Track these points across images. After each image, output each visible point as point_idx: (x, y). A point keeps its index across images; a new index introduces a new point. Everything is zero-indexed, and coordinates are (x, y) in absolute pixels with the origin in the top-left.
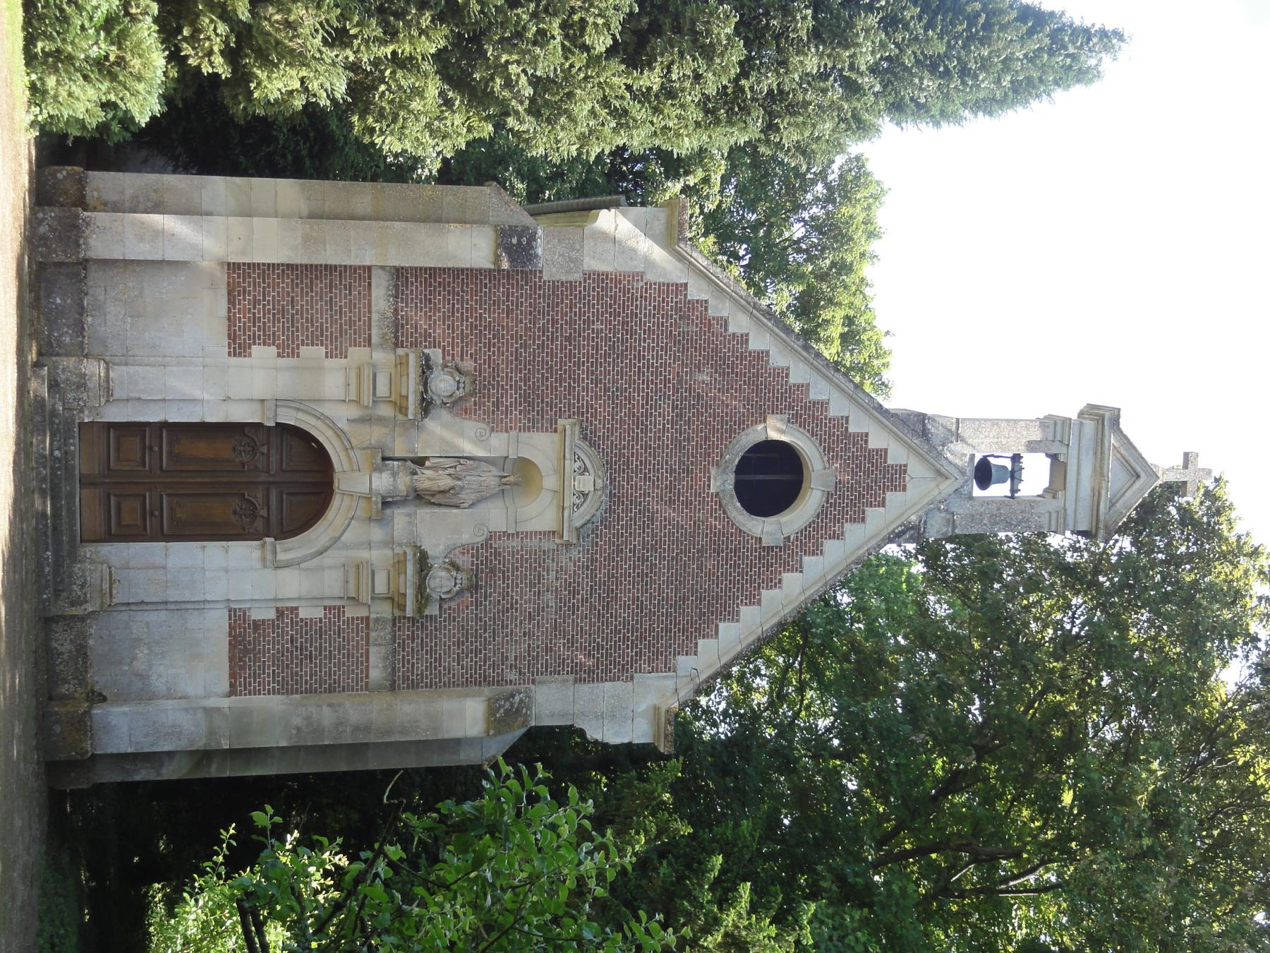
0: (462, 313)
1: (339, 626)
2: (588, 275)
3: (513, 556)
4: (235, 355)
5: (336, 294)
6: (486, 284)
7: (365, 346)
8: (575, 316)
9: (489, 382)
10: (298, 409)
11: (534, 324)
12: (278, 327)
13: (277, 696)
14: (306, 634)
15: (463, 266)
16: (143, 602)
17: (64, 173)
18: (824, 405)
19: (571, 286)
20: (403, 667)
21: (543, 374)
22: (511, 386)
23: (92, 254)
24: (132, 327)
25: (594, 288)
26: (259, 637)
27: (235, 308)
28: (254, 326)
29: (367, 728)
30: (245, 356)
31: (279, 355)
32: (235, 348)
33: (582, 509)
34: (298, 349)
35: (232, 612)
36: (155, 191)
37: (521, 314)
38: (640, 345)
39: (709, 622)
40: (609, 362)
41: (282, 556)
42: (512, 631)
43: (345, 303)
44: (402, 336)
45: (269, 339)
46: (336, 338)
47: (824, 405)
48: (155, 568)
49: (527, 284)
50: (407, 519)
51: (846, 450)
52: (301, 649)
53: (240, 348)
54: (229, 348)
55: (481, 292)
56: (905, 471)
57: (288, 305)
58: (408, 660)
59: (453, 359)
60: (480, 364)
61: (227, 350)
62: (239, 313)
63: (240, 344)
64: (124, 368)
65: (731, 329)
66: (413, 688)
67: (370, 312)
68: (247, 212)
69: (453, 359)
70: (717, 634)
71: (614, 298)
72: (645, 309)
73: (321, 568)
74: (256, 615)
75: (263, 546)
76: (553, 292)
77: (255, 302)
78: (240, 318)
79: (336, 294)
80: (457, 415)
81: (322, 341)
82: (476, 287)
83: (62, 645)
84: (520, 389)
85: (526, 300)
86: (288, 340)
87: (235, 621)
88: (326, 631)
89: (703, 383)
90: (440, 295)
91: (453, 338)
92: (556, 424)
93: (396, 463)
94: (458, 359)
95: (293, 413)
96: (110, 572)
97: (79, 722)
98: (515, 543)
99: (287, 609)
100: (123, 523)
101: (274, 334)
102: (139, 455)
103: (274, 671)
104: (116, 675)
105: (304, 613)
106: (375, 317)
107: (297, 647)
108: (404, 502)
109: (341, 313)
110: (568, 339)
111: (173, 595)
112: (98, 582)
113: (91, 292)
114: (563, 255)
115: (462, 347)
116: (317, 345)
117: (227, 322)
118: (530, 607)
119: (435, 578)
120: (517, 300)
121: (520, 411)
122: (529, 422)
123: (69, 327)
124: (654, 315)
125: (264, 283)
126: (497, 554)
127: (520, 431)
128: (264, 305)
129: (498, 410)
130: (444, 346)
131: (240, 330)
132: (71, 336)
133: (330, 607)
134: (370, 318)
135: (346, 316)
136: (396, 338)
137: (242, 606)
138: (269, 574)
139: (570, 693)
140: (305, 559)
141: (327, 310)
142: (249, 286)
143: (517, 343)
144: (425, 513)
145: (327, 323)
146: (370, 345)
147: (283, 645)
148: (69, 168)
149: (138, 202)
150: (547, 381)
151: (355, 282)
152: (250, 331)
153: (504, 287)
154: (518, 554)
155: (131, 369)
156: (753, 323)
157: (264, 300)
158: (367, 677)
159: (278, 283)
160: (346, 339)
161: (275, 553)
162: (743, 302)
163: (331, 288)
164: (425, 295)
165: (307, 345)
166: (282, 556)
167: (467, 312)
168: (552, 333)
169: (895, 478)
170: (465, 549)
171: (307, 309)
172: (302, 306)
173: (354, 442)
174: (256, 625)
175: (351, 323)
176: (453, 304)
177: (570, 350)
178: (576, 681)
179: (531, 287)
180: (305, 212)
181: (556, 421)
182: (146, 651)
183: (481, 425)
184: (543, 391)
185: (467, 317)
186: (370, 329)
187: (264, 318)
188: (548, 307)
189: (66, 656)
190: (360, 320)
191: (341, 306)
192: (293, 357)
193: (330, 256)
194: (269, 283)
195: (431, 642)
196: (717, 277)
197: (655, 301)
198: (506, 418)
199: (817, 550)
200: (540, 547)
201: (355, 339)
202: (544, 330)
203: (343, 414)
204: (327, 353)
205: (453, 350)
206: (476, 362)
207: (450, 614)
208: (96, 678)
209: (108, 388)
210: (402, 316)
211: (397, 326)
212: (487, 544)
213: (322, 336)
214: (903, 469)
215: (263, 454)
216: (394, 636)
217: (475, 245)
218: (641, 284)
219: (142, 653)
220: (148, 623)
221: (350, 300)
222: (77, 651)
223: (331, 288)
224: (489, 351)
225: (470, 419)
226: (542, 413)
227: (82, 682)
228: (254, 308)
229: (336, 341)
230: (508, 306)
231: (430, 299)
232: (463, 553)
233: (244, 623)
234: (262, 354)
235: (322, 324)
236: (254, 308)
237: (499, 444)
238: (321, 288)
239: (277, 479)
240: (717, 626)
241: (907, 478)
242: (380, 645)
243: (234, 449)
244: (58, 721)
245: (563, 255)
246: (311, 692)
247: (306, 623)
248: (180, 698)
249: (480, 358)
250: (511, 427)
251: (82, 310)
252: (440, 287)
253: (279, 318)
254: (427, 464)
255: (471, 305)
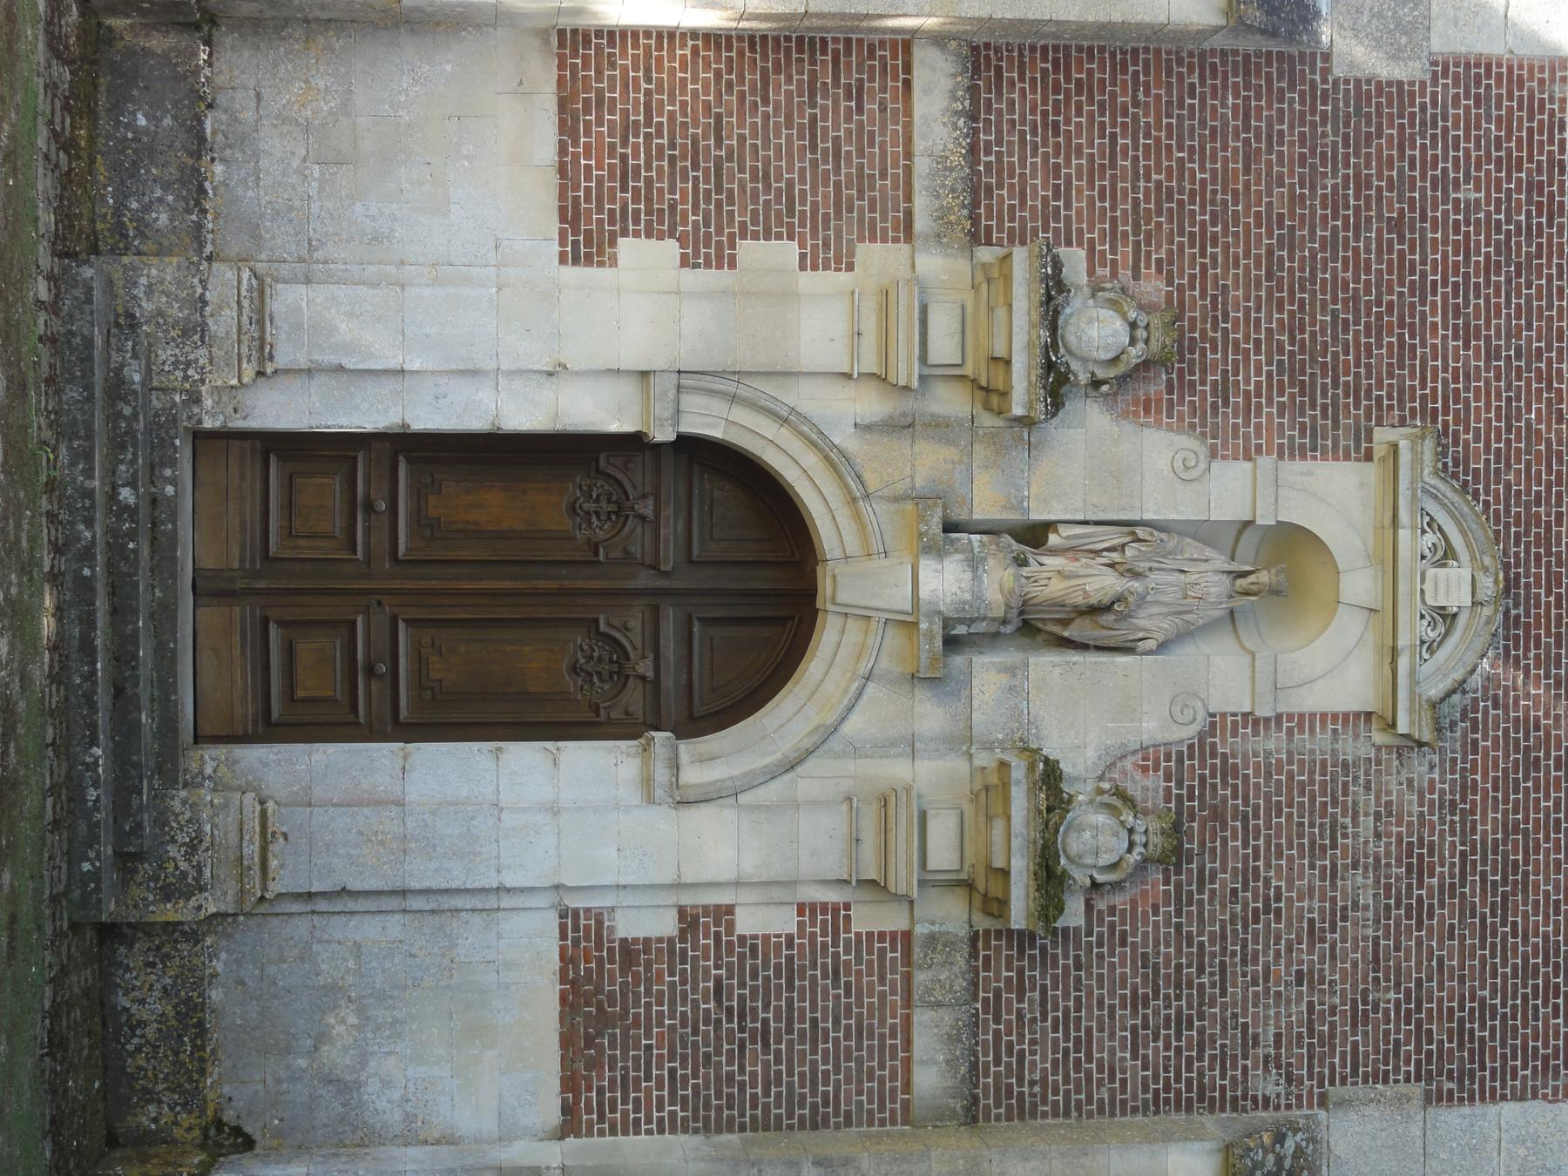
0: (1136, 158)
1: (836, 955)
2: (1441, 67)
3: (1269, 775)
4: (576, 261)
5: (824, 109)
7: (896, 240)
8: (1412, 167)
9: (1203, 332)
10: (733, 398)
11: (1313, 188)
12: (684, 192)
13: (682, 1138)
16: (344, 892)
19: (1400, 92)
20: (997, 1062)
21: (1335, 314)
22: (1257, 342)
24: (321, 189)
25: (1456, 97)
26: (637, 983)
27: (575, 144)
28: (624, 189)
30: (601, 264)
31: (684, 262)
32: (575, 244)
33: (1442, 654)
34: (733, 246)
35: (569, 920)
37: (1281, 163)
43: (849, 132)
44: (989, 217)
45: (661, 222)
46: (826, 217)
48: (379, 803)
49: (1292, 88)
50: (1004, 679)
52: (742, 1017)
53: (588, 243)
54: (563, 243)
55: (1181, 107)
57: (706, 137)
58: (1010, 1045)
59: (1114, 274)
60: (1181, 288)
62: (588, 156)
63: (588, 233)
66: (1021, 1117)
67: (909, 155)
69: (1114, 274)
71: (1506, 123)
76: (1358, 108)
78: (588, 168)
79: (824, 109)
80: (1125, 415)
81: (791, 226)
82: (1169, 93)
84: (1281, 351)
85: (1291, 127)
86: (707, 224)
87: (576, 942)
88: (802, 969)
90: (1079, 113)
91: (1114, 220)
92: (1369, 439)
94: (1125, 274)
95: (718, 407)
96: (264, 814)
98: (1274, 742)
99: (706, 910)
100: (300, 694)
101: (672, 207)
103: (672, 1071)
104: (278, 1081)
105: (747, 923)
106: (921, 165)
107: (730, 1010)
108: (993, 639)
109: (837, 156)
110: (1397, 225)
111: (422, 872)
112: (233, 838)
113: (222, 100)
115: (1137, 244)
116: (779, 237)
118: (1312, 908)
119: (1081, 829)
120: (1270, 126)
121: (1281, 406)
123: (166, 187)
126: (1228, 771)
127: (1281, 456)
128: (648, 136)
129: (1226, 404)
130: (1091, 242)
131: (588, 199)
132: (172, 209)
133: (813, 907)
134: (908, 170)
135: (849, 164)
136: (974, 219)
137: (595, 902)
138: (662, 822)
141: (802, 149)
143: (1270, 235)
145: (803, 181)
150: (1346, 330)
152: (612, 200)
153: (1236, 95)
157: (648, 123)
159: (683, 81)
160: (850, 221)
161: (675, 766)
163: (812, 95)
164: (1045, 114)
165: (755, 236)
166: (693, 777)
168: (1357, 209)
170: (1150, 757)
171: (754, 147)
172: (742, 138)
173: (873, 483)
174: (630, 952)
176: (1113, 136)
177: (1401, 253)
178: (1428, 1100)
179: (1302, 94)
181: (1369, 432)
182: (353, 1020)
184: (1335, 355)
186: (909, 198)
187: (649, 168)
188: (1346, 145)
189: (150, 1031)
190: (883, 176)
192: (720, 267)
195: (1066, 996)
198: (1247, 424)
201: (873, 222)
202: (1335, 203)
204: (803, 257)
205: (1114, 251)
206: (1170, 283)
207: (1112, 926)
208: (226, 1089)
209: (262, 339)
210: (988, 165)
211: (976, 192)
212: (1201, 746)
213: (791, 213)
215: (643, 518)
216: (974, 984)
219: (342, 1025)
221: (860, 125)
223: (812, 95)
224: (1203, 254)
225: (1159, 424)
226: (1333, 412)
227: (191, 1097)
228: (624, 144)
230: (1247, 142)
231: (1056, 124)
232: (1145, 769)
233: (599, 947)
235: (790, 184)
236: (624, 144)
238: (789, 94)
239: (678, 584)
242: (939, 1005)
243: (572, 509)
246: (766, 1128)
248: (438, 1142)
249: (1181, 270)
250: (1259, 449)
251: (199, 144)
252: (1079, 93)
253: (684, 170)
254: (1053, 539)
255: (1158, 140)
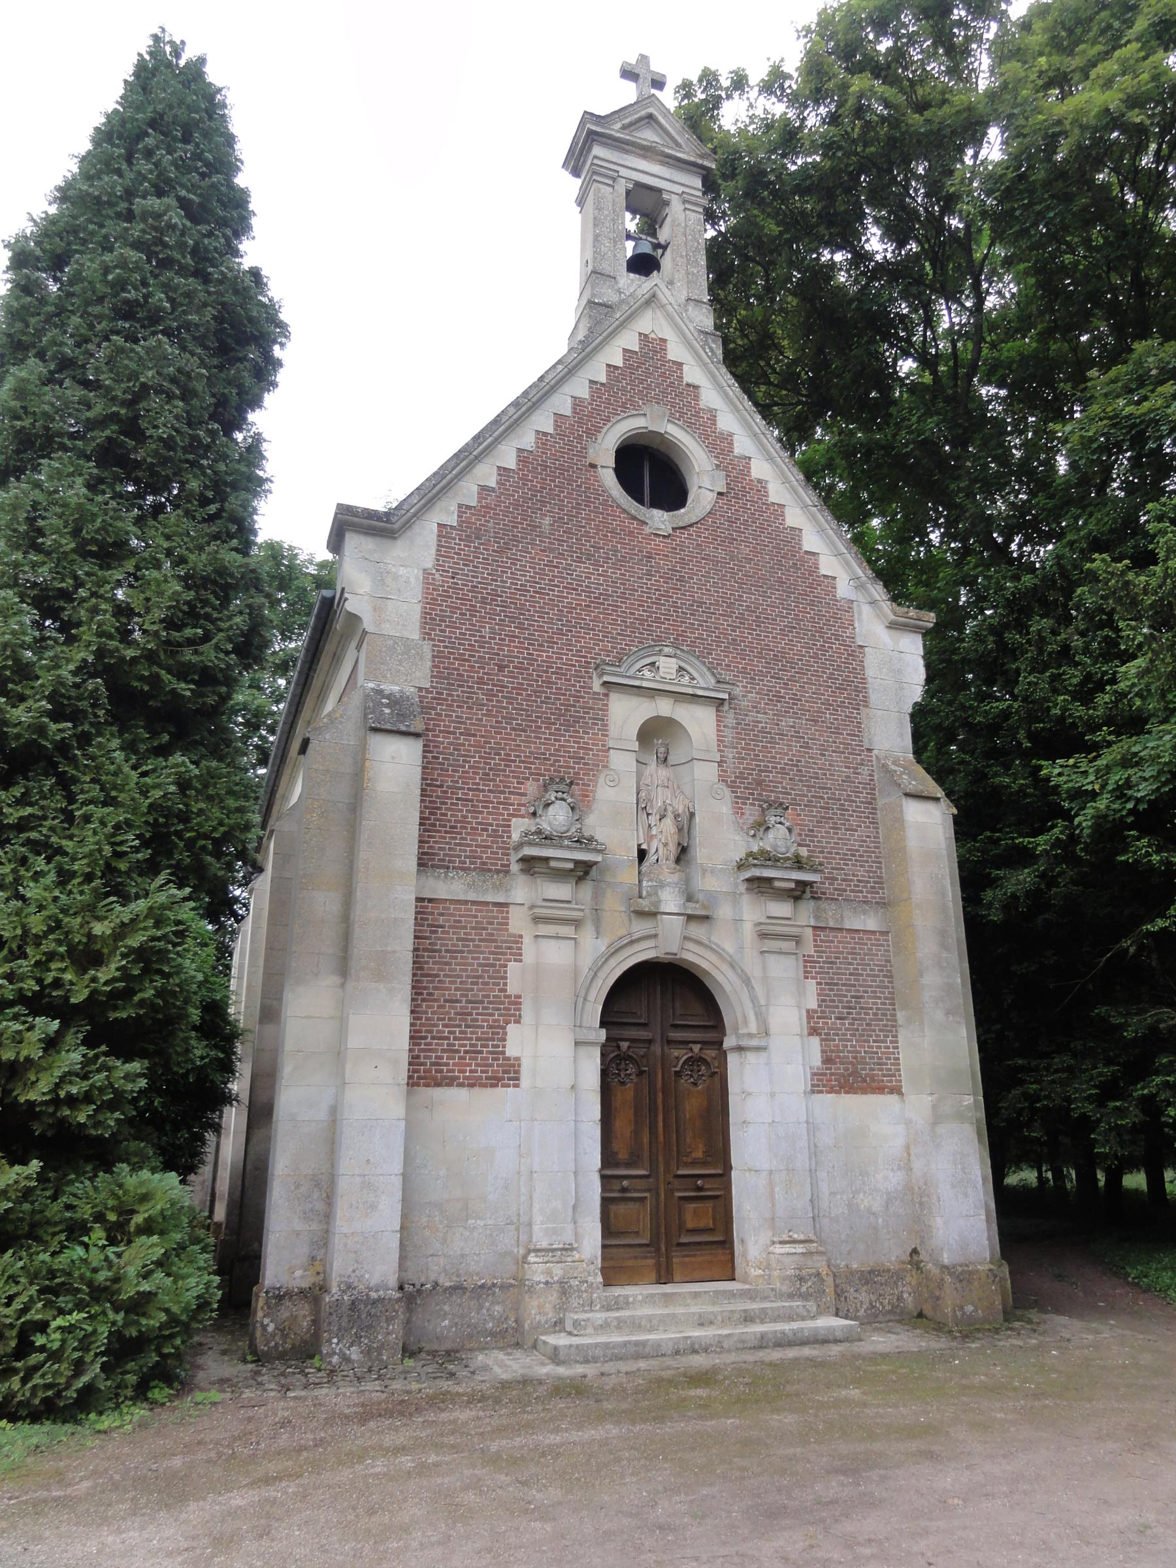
0: (469, 789)
1: (824, 962)
2: (426, 635)
3: (743, 758)
4: (517, 1079)
5: (442, 945)
6: (434, 757)
7: (508, 912)
8: (473, 656)
9: (551, 765)
10: (585, 999)
11: (483, 705)
12: (483, 1021)
13: (900, 1038)
14: (834, 1001)
15: (419, 777)
16: (811, 1201)
17: (266, 1321)
18: (577, 402)
19: (437, 656)
20: (861, 892)
21: (542, 702)
22: (556, 740)
23: (393, 1281)
24: (480, 1218)
25: (441, 631)
26: (839, 1057)
27: (458, 1078)
28: (481, 1052)
29: (943, 933)
30: (519, 1066)
31: (518, 1022)
32: (509, 1079)
33: (695, 674)
34: (509, 997)
35: (815, 1089)
36: (297, 1187)
37: (471, 719)
38: (509, 588)
39: (801, 559)
40: (529, 625)
41: (753, 1027)
42: (820, 769)
43: (454, 933)
44: (496, 864)
45: (498, 1033)
46: (496, 947)
47: (577, 402)
48: (771, 1185)
49: (434, 709)
50: (708, 875)
51: (624, 389)
52: (850, 1008)
53: (508, 1072)
54: (508, 1086)
55: (443, 764)
56: (646, 336)
57: (455, 1008)
58: (855, 886)
59: (523, 805)
60: (531, 774)
61: (511, 1089)
62: (464, 1071)
63: (504, 1072)
64: (536, 1228)
65: (492, 483)
66: (882, 883)
67: (466, 902)
68: (338, 1054)
69: (523, 805)
70: (813, 554)
71: (453, 609)
72: (467, 575)
73: (765, 979)
74: (817, 1060)
75: (740, 1049)
76: (445, 678)
77: (452, 1051)
78: (471, 1071)
79: (442, 945)
80: (589, 806)
81: (501, 966)
82: (437, 769)
83: (861, 1302)
84: (559, 730)
85: (454, 711)
86: (499, 1009)
87: (824, 1086)
88: (830, 978)
89: (552, 525)
90: (446, 815)
91: (498, 803)
92: (598, 694)
93: (645, 883)
94: (524, 800)
95: (589, 1006)
96: (781, 1243)
97: (961, 1281)
98: (730, 754)
99: (809, 1023)
100: (711, 1226)
101: (491, 1027)
102: (632, 1206)
103: (874, 1041)
104: (889, 1232)
105: (813, 1004)
106: (472, 896)
107: (848, 1013)
108: (687, 881)
109: (467, 940)
110: (501, 668)
111: (802, 1161)
112: (795, 1258)
113: (433, 1277)
114: (401, 662)
115: (510, 793)
116: (506, 972)
117: (477, 1089)
118: (796, 746)
119: (776, 846)
120: (453, 722)
121: (584, 732)
122: (597, 724)
123: (481, 1307)
124: (474, 566)
125: (425, 1038)
126: (741, 776)
127: (607, 736)
128: (455, 1039)
129: (583, 758)
130: (509, 815)
131: (487, 1072)
132: (492, 1303)
133: (805, 972)
134: (474, 903)
135: (469, 934)
136: (498, 872)
137: (809, 1076)
138: (775, 1043)
139: (879, 713)
140: (754, 1000)
141: (462, 958)
142: (430, 1057)
143: (506, 728)
144: (701, 854)
145: (478, 958)
146: (506, 905)
147: (846, 1029)
148: (260, 1314)
149: (312, 1210)
150: (550, 698)
151: (427, 919)
152: (487, 1059)
153: (438, 736)
154: (741, 753)
155: (538, 1219)
156: (485, 460)
157: (448, 1038)
158: (873, 932)
159: (427, 1019)
160: (498, 935)
161: (750, 1036)
162: (464, 463)
163: (435, 951)
164: (446, 832)
165: (505, 984)
166: (753, 1027)
167: (467, 784)
168: (493, 685)
169: (652, 347)
170: (738, 811)
171: (461, 983)
172: (457, 989)
173: (623, 932)
174: (827, 1060)
175: (478, 928)
176: (458, 799)
177: (514, 667)
178: (867, 706)
179: (438, 704)
180: (335, 979)
181: (595, 693)
182: (861, 1196)
183: (601, 780)
184: (561, 704)
185: (473, 784)
186: (487, 903)
187: (471, 1039)
188: (462, 686)
189: (873, 1297)
190: (476, 917)
191: (458, 940)
192: (520, 1003)
193: (403, 945)
194: (426, 1031)
195: (834, 858)
196: (435, 486)
197: (458, 564)
198: (592, 750)
199: (728, 438)
200: (733, 728)
201: (498, 924)
202: (490, 694)
203: (592, 945)
204: (515, 960)
205: (513, 805)
206: (528, 779)
207: (806, 835)
208: (893, 1259)
209: (562, 1250)
210: (471, 863)
211: (484, 870)
212: (732, 786)
213: (493, 965)
214: (644, 337)
215: (629, 1047)
216: (832, 899)
217: (393, 758)
218: (437, 576)
219: (864, 1202)
220: (831, 1193)
221: (450, 927)
222: (867, 1283)
223: (435, 951)
224: (515, 761)
225: (594, 791)
226: (587, 709)
227: (896, 1277)
228: (458, 1051)
229: (501, 947)
230: (461, 734)
231: (451, 827)
232: (742, 814)
233: (825, 1074)
234: (517, 1041)
235: (480, 965)
236: (458, 1051)
237: (623, 762)
238: (434, 963)
239: (659, 1030)
240: (807, 552)
241: (653, 336)
242: (842, 917)
243: (623, 1083)
244: (961, 1308)
245: (401, 662)
246: (893, 999)
247: (823, 1001)
248: (909, 1154)
249: (522, 773)
250: (603, 745)
251: (459, 1288)
252: (435, 814)
253: (472, 1020)
254: (644, 847)
255: (459, 777)
